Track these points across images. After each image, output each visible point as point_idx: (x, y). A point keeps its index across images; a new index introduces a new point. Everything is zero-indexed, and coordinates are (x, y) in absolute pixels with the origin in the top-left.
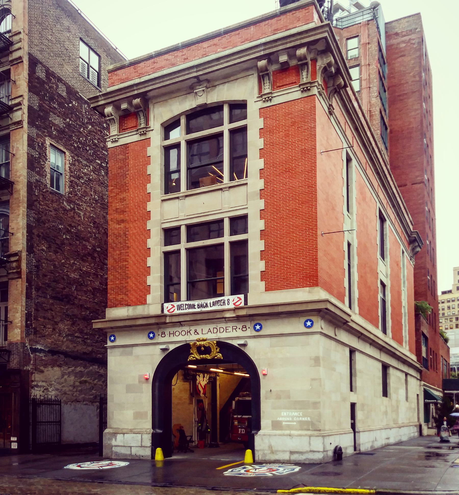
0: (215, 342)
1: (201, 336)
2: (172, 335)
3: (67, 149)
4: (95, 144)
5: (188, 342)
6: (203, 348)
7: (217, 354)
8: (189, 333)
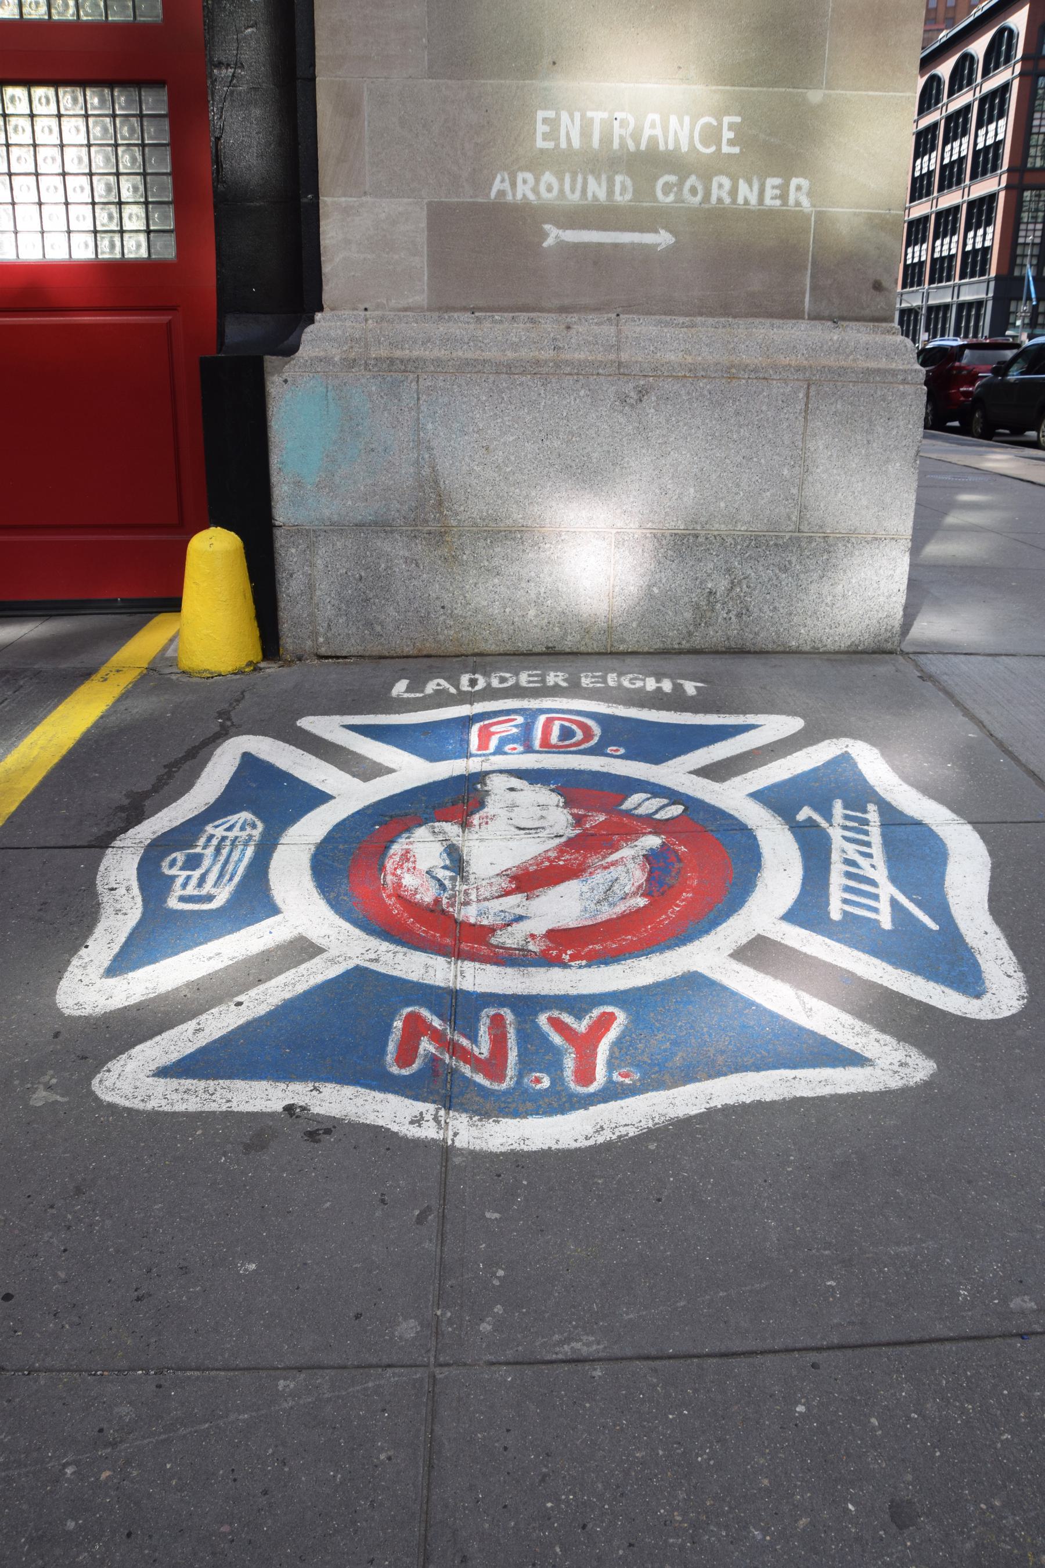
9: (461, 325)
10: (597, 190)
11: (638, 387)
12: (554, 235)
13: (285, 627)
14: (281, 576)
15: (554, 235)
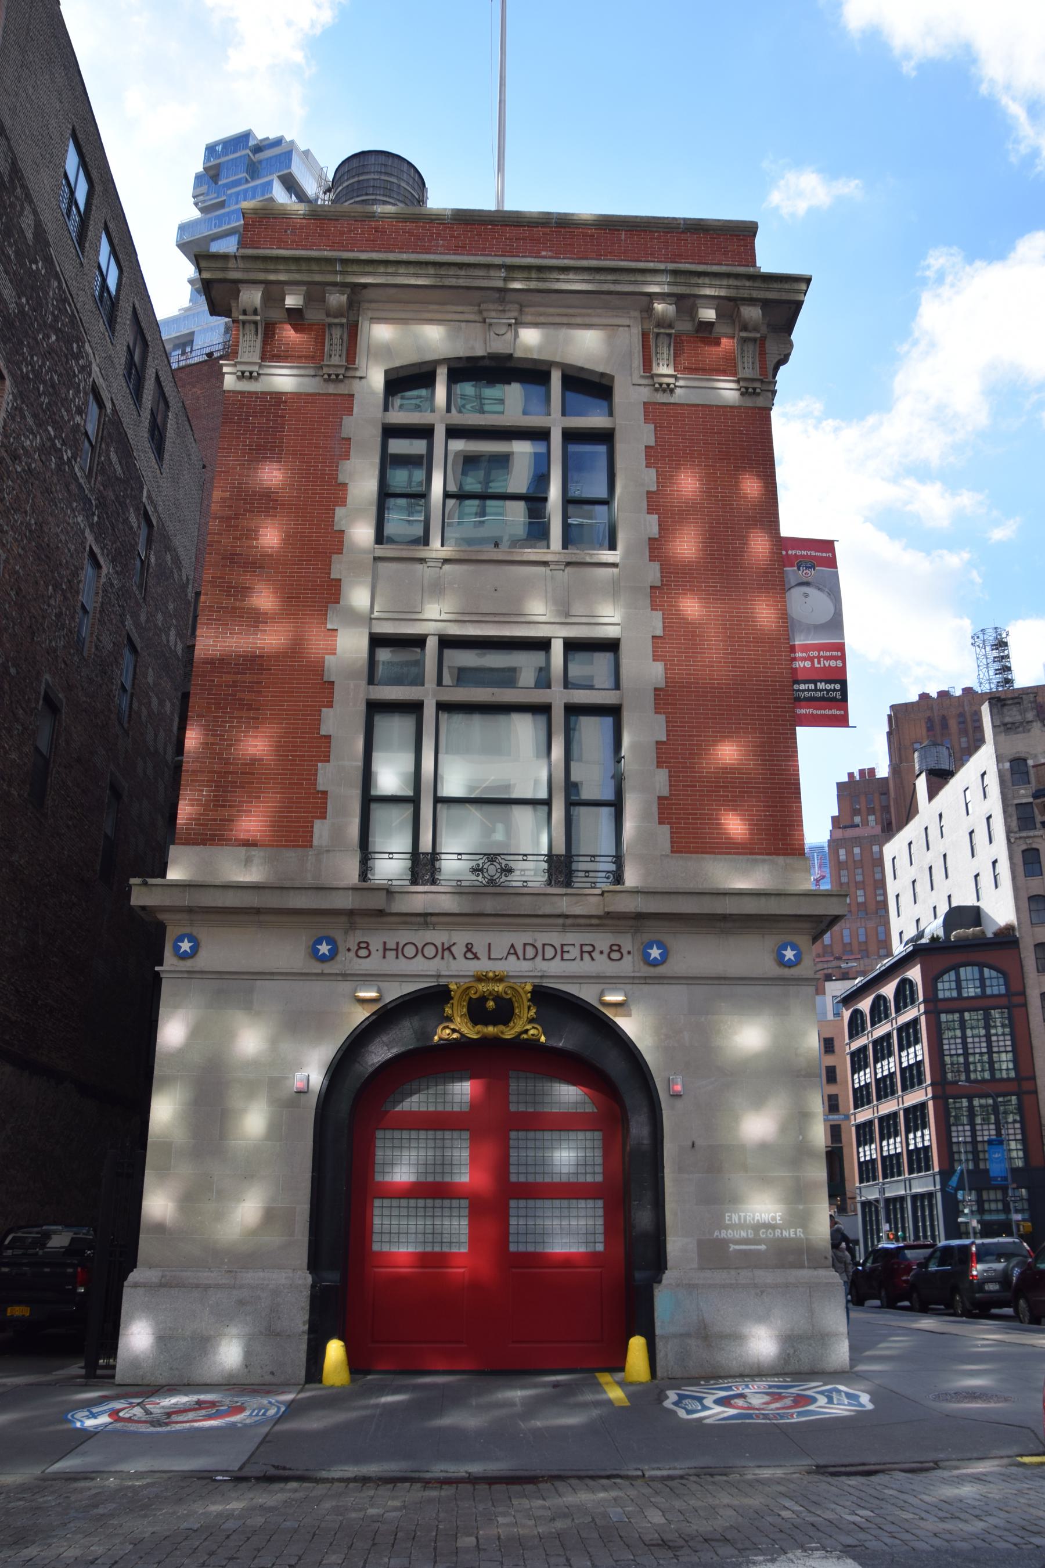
0: (529, 988)
2: (391, 955)
3: (10, 372)
4: (53, 386)
5: (443, 981)
6: (491, 1004)
7: (528, 1027)
8: (446, 953)
9: (708, 1274)
10: (743, 1234)
11: (760, 1290)
12: (732, 1247)
13: (658, 1369)
14: (657, 1351)
15: (732, 1247)
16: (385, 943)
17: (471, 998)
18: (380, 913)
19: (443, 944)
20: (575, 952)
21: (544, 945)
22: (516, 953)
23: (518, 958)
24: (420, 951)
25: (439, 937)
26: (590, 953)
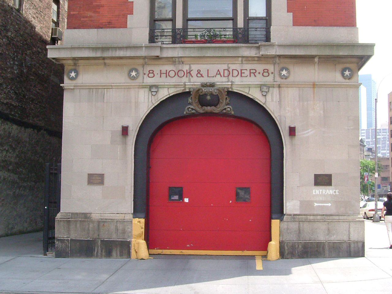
1: (206, 80)
6: (209, 98)
7: (226, 107)
8: (188, 74)
16: (161, 71)
17: (200, 95)
18: (157, 58)
19: (187, 70)
20: (247, 73)
21: (233, 70)
22: (220, 74)
23: (221, 76)
24: (177, 74)
25: (186, 68)
26: (254, 73)
